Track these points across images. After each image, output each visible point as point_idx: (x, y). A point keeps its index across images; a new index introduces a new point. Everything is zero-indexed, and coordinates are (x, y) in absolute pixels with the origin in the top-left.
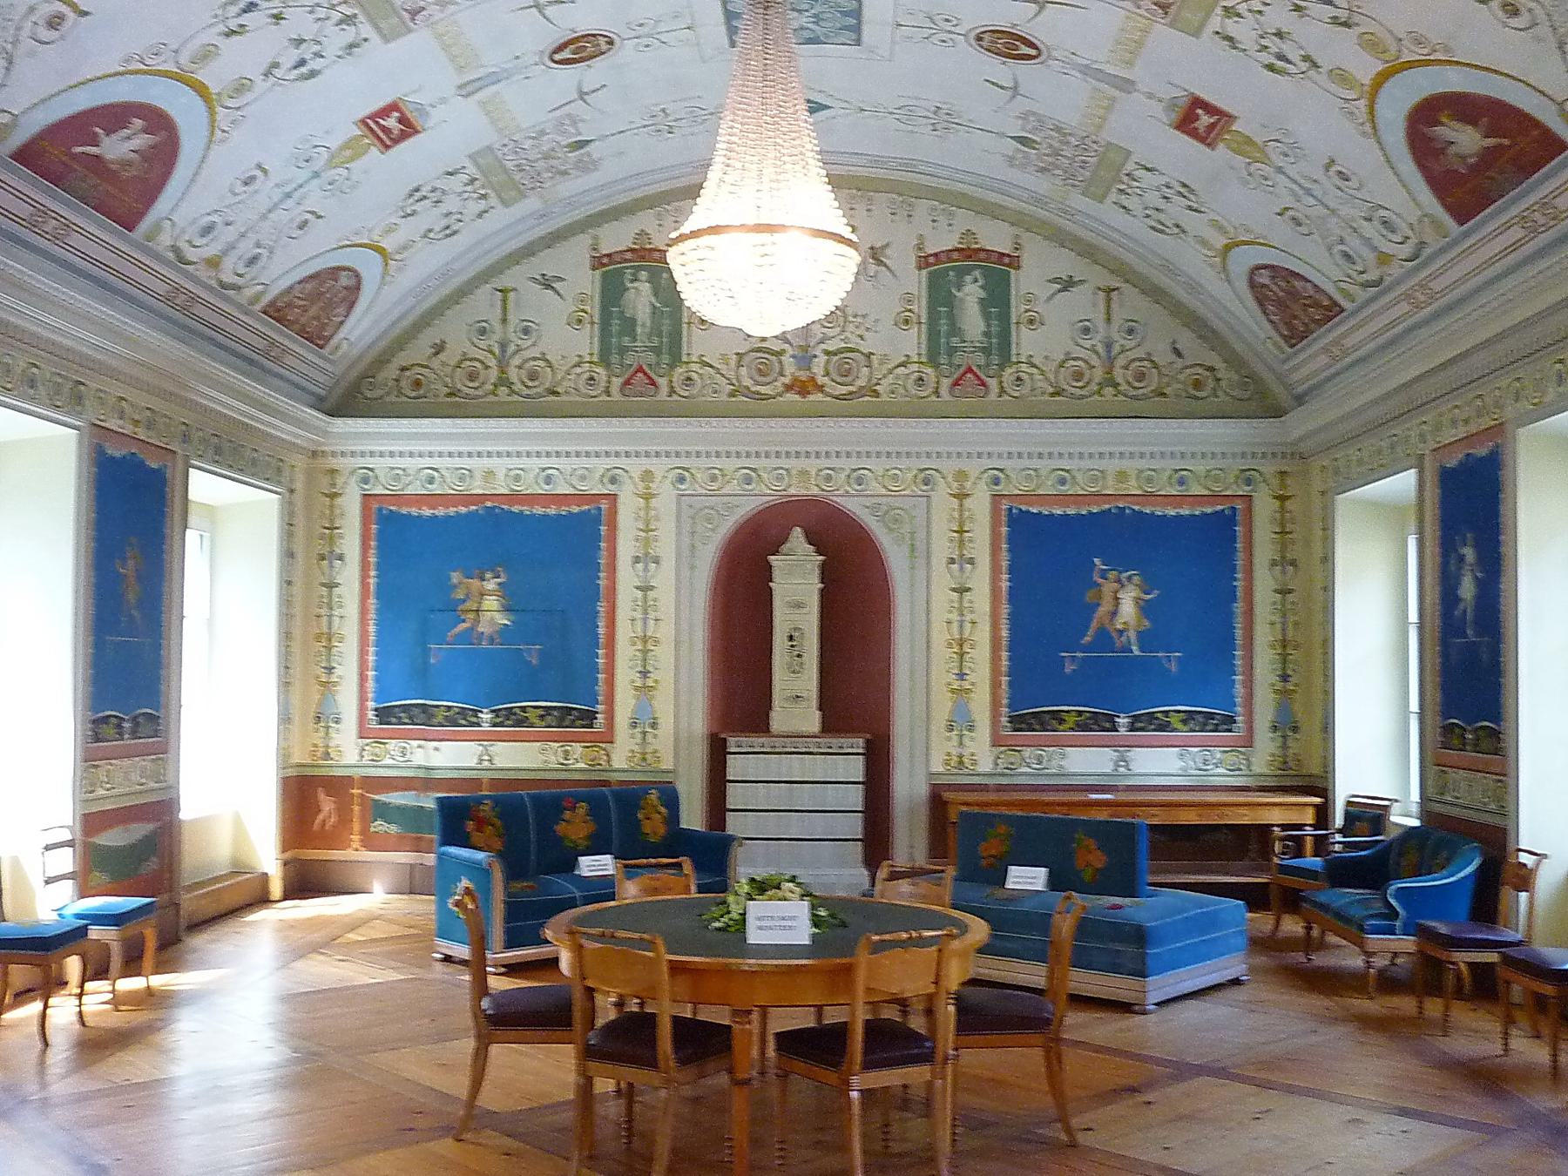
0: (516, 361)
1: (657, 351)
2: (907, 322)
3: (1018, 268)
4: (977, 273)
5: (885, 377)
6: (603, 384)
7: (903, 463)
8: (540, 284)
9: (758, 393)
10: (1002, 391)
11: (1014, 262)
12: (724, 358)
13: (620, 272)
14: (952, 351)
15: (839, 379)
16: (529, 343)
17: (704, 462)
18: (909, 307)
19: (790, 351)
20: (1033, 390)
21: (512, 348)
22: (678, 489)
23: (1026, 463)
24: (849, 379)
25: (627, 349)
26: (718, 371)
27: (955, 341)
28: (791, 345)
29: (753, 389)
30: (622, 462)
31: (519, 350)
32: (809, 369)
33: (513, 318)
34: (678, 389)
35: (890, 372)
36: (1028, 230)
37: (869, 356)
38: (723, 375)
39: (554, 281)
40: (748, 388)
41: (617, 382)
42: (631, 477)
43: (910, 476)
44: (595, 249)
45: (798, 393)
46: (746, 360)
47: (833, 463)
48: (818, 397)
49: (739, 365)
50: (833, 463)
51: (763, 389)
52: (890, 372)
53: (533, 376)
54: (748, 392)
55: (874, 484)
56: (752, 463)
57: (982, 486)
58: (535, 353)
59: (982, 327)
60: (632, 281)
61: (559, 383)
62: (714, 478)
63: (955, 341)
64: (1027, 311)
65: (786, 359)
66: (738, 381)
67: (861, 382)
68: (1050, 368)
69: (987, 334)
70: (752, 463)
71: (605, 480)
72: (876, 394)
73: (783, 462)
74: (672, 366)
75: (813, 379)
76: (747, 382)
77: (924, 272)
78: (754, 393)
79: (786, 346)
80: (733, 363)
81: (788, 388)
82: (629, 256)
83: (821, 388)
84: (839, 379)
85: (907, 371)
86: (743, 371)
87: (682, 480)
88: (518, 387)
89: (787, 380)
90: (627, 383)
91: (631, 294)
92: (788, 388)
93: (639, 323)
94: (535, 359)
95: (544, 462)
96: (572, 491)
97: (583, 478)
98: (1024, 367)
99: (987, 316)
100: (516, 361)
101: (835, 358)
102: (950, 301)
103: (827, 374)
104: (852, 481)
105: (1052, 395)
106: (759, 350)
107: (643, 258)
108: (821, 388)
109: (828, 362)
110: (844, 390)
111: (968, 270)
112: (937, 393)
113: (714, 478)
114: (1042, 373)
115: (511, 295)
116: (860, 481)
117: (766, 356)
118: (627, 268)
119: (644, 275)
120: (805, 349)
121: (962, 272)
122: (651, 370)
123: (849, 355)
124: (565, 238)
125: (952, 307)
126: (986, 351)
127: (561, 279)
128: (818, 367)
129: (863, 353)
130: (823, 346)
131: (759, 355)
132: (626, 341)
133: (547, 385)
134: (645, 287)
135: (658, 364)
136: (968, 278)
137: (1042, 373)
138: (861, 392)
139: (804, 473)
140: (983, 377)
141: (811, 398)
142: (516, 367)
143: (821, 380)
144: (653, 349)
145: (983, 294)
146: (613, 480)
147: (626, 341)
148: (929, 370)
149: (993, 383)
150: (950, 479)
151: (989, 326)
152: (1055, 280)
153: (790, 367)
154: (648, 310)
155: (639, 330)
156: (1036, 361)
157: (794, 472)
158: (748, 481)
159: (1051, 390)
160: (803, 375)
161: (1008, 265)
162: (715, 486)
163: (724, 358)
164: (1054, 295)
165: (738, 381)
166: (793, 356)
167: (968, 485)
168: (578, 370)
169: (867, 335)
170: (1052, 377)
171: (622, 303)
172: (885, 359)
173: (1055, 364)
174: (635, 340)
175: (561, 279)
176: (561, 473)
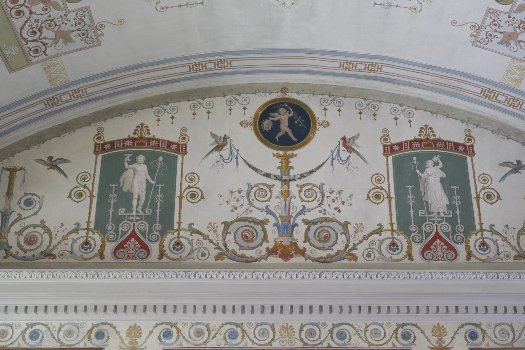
0: (17, 227)
1: (151, 220)
2: (377, 197)
3: (473, 154)
4: (436, 158)
5: (361, 242)
6: (98, 248)
7: (383, 318)
8: (48, 165)
9: (243, 256)
10: (469, 255)
11: (469, 150)
12: (212, 227)
13: (122, 156)
14: (420, 221)
15: (321, 245)
16: (31, 212)
17: (191, 318)
18: (379, 185)
19: (272, 220)
20: (498, 254)
21: (13, 217)
22: (165, 344)
23: (500, 317)
24: (327, 245)
25: (122, 218)
26: (206, 238)
27: (422, 213)
28: (274, 215)
29: (239, 253)
30: (110, 317)
31: (20, 218)
32: (291, 235)
33: (18, 192)
34: (168, 252)
35: (365, 238)
36: (477, 126)
37: (345, 225)
38: (211, 241)
39: (60, 163)
40: (233, 251)
41: (110, 247)
42: (118, 333)
43: (390, 331)
44: (99, 138)
45: (280, 256)
46: (232, 228)
47: (316, 317)
48: (298, 259)
49: (226, 232)
50: (316, 317)
51: (249, 253)
52: (365, 238)
53: (31, 240)
54: (233, 256)
55: (355, 338)
56: (238, 318)
57: (460, 339)
58: (36, 220)
59: (446, 201)
60: (130, 163)
61: (55, 247)
62: (199, 333)
63: (422, 213)
64: (484, 188)
65: (270, 228)
66: (225, 245)
67: (340, 246)
68: (511, 235)
69: (451, 206)
70: (238, 318)
71: (93, 335)
72: (355, 258)
73: (268, 317)
74: (163, 233)
75: (294, 244)
76: (232, 246)
77: (390, 158)
78: (239, 256)
79: (270, 217)
80: (220, 229)
81: (271, 252)
82: (129, 143)
83: (302, 252)
84: (321, 245)
85: (381, 238)
86: (230, 237)
87: (167, 334)
88: (15, 249)
89: (271, 245)
90: (121, 246)
91: (129, 173)
92: (271, 252)
93: (136, 196)
94: (35, 226)
95: (32, 317)
96: (57, 345)
97: (70, 333)
98: (487, 234)
99: (449, 193)
100: (17, 227)
101: (313, 228)
102: (415, 181)
103: (307, 239)
104: (334, 336)
105: (515, 258)
106: (245, 219)
107: (140, 145)
108: (302, 252)
109: (308, 230)
110: (324, 254)
111: (430, 156)
112: (409, 255)
113: (199, 333)
114: (505, 239)
115: (19, 175)
116: (342, 335)
117: (252, 224)
118: (128, 152)
119: (141, 158)
120: (287, 219)
121: (423, 159)
122: (145, 237)
123: (324, 224)
124: (74, 130)
125: (417, 185)
126: (452, 221)
127: (65, 161)
128: (299, 234)
129: (340, 223)
130: (302, 217)
131: (247, 223)
132: (121, 211)
133: (44, 248)
134: (142, 169)
135: (151, 231)
136: (430, 163)
137: (505, 239)
138: (339, 256)
139: (287, 328)
140: (452, 243)
141: (292, 260)
142: (16, 233)
143: (301, 245)
144: (147, 219)
145: (443, 175)
146: (100, 335)
147: (121, 211)
148: (401, 237)
149: (461, 248)
150: (429, 333)
151: (451, 200)
152: (505, 164)
153: (273, 234)
154: (144, 186)
155: (135, 202)
156: (499, 228)
157: (277, 328)
158: (233, 335)
159: (514, 253)
160: (286, 241)
161: (465, 151)
162: (201, 340)
163: (212, 227)
164: (505, 176)
165: (225, 245)
166: (275, 225)
167: (447, 339)
168: (74, 236)
169: (342, 207)
170: (514, 243)
171: (121, 180)
172: (359, 227)
173: (517, 231)
174: (129, 209)
175: (65, 161)
176: (49, 329)
